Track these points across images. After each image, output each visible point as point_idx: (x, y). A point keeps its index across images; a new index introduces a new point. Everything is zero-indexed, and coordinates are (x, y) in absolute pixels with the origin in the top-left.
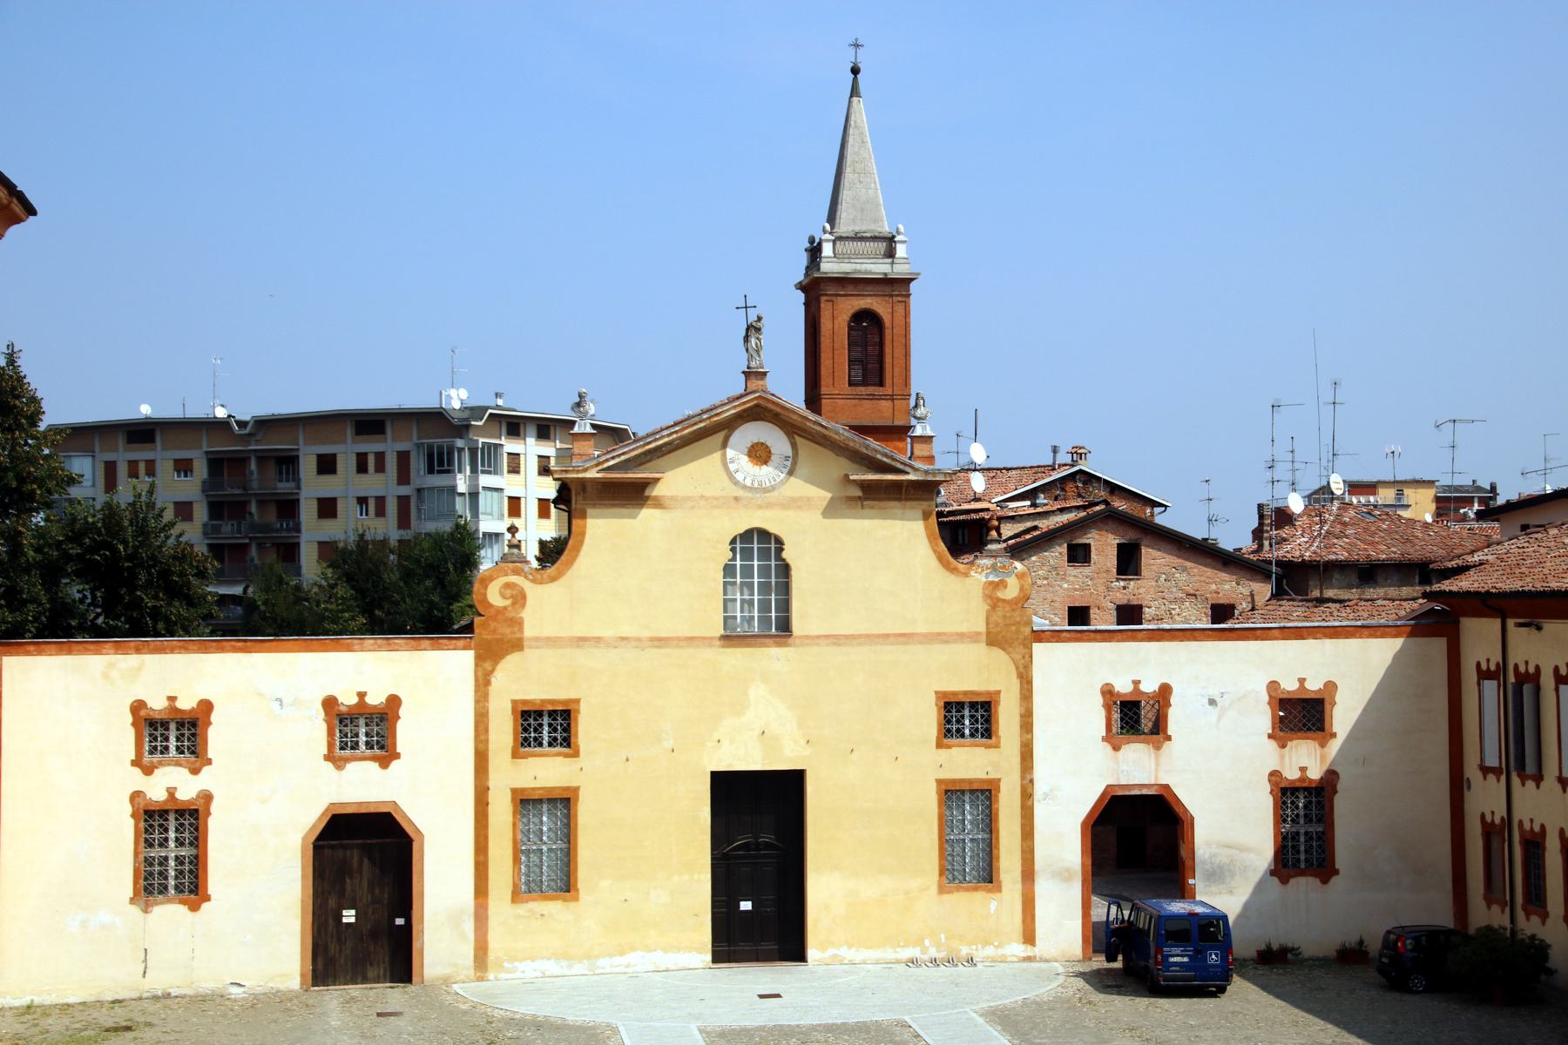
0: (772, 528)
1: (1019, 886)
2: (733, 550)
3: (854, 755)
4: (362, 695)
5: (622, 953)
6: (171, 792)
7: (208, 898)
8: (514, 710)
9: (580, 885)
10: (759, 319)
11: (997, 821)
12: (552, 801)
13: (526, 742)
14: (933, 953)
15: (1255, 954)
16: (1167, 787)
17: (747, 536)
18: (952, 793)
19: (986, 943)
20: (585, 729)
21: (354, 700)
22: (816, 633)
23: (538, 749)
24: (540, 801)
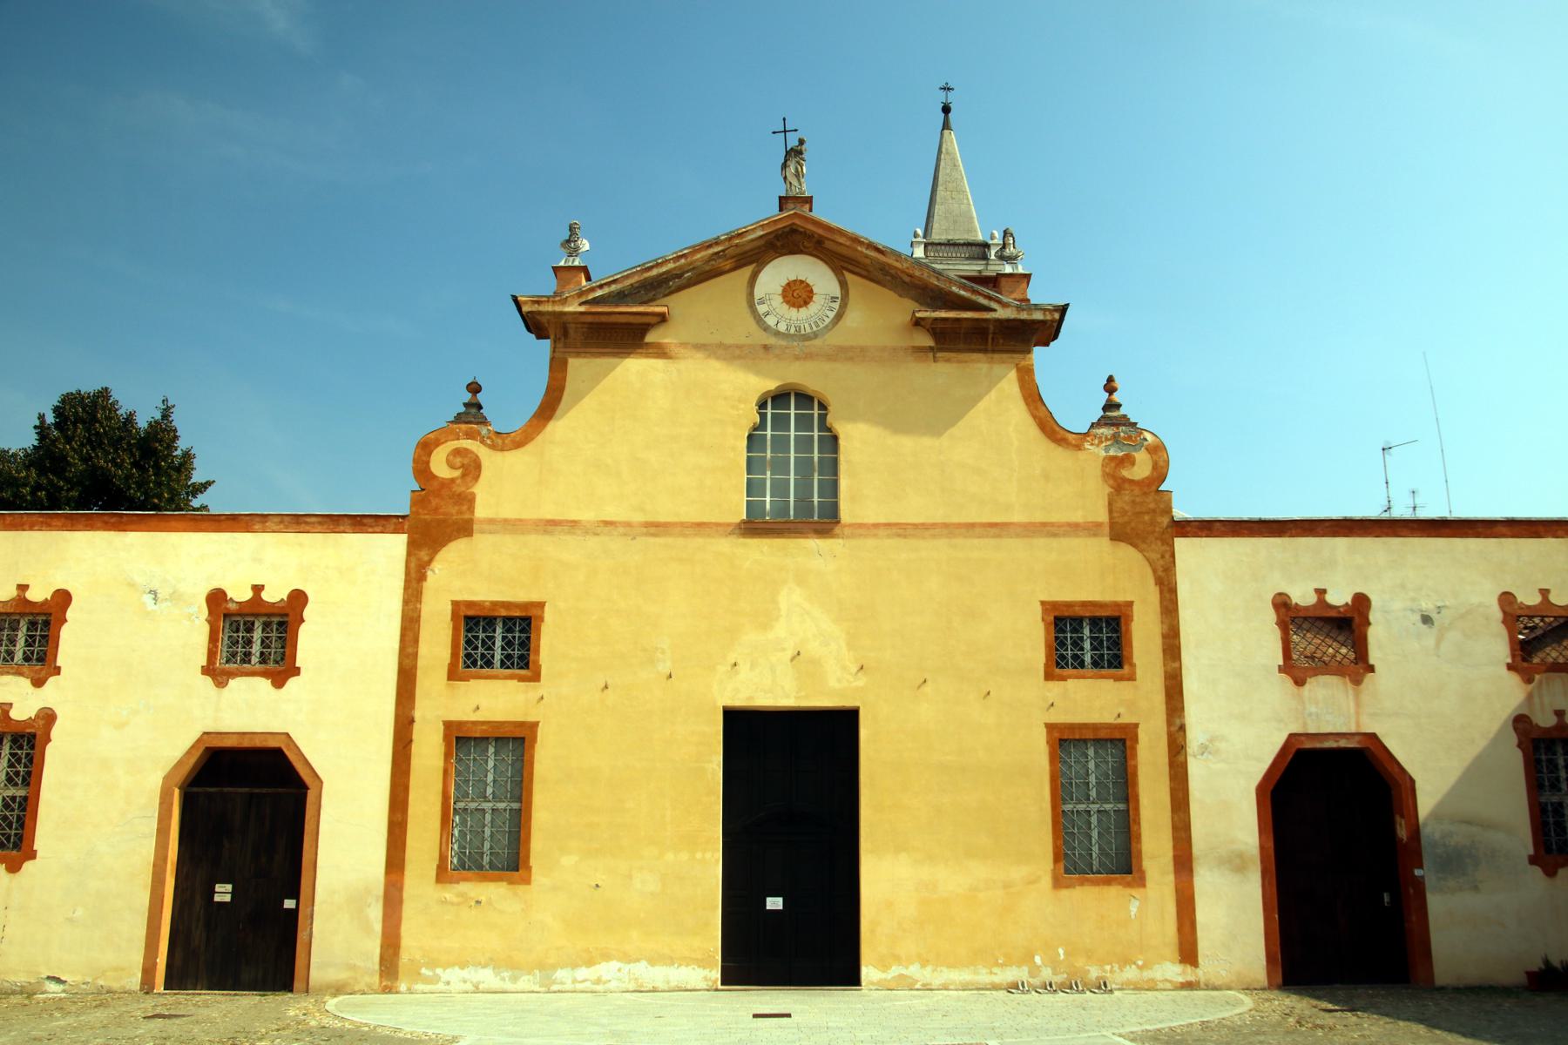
0: (812, 384)
1: (1171, 878)
2: (763, 417)
3: (927, 689)
4: (257, 589)
5: (590, 963)
7: (32, 855)
8: (455, 615)
9: (533, 862)
10: (801, 142)
11: (1135, 784)
12: (500, 741)
13: (471, 661)
14: (1047, 974)
15: (1523, 979)
16: (1373, 737)
17: (779, 398)
18: (1067, 742)
19: (1126, 961)
20: (550, 643)
21: (247, 595)
22: (872, 520)
23: (486, 670)
24: (482, 741)
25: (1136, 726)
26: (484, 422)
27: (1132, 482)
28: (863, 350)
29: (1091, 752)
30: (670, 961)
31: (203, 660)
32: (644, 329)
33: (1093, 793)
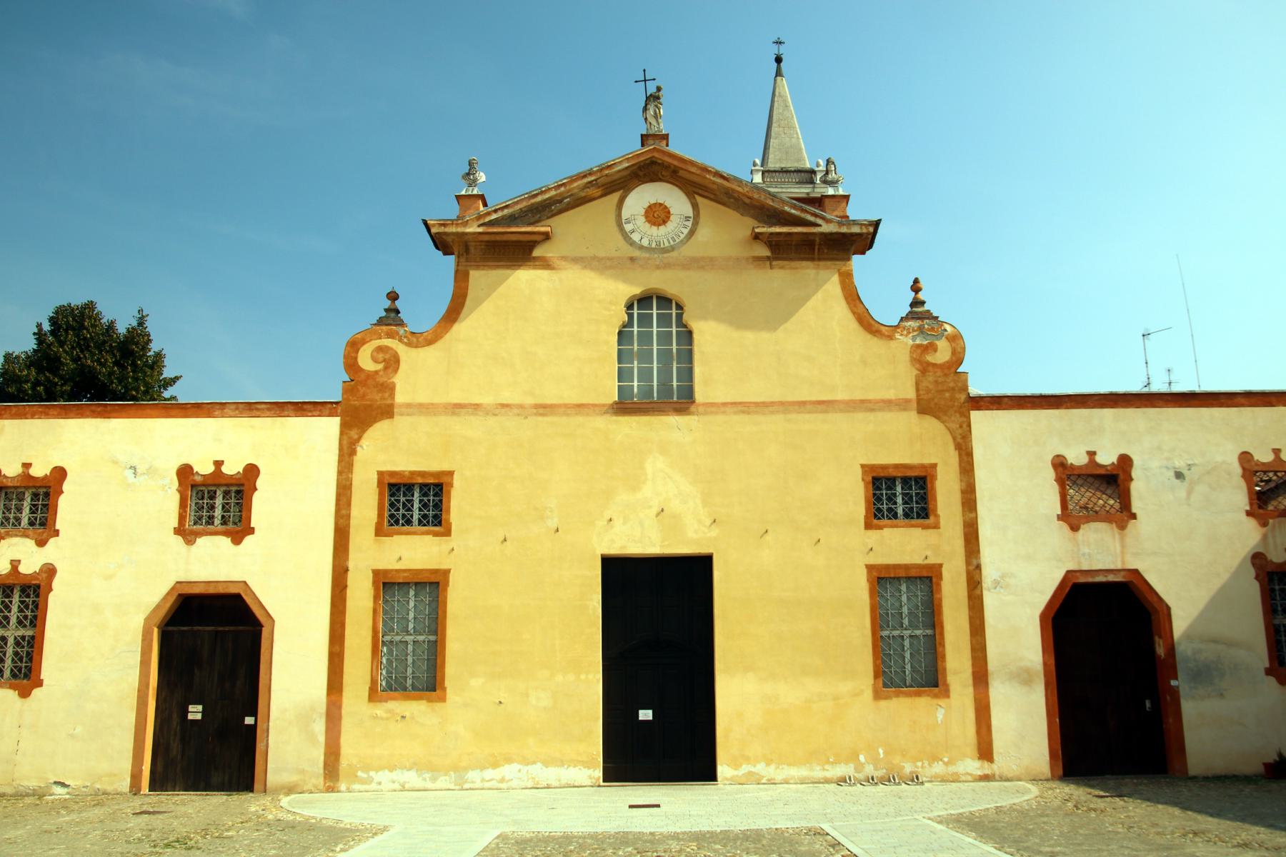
1: (970, 690)
2: (631, 316)
3: (768, 537)
4: (218, 464)
5: (495, 765)
6: (15, 564)
8: (380, 483)
9: (447, 684)
10: (659, 89)
11: (940, 613)
13: (394, 521)
14: (869, 770)
15: (1261, 769)
16: (1136, 572)
17: (644, 300)
19: (934, 758)
20: (458, 505)
21: (210, 469)
22: (721, 399)
23: (406, 528)
25: (941, 566)
26: (401, 323)
27: (934, 365)
28: (712, 259)
29: (904, 588)
30: (561, 763)
31: (175, 523)
32: (532, 245)
33: (906, 622)
